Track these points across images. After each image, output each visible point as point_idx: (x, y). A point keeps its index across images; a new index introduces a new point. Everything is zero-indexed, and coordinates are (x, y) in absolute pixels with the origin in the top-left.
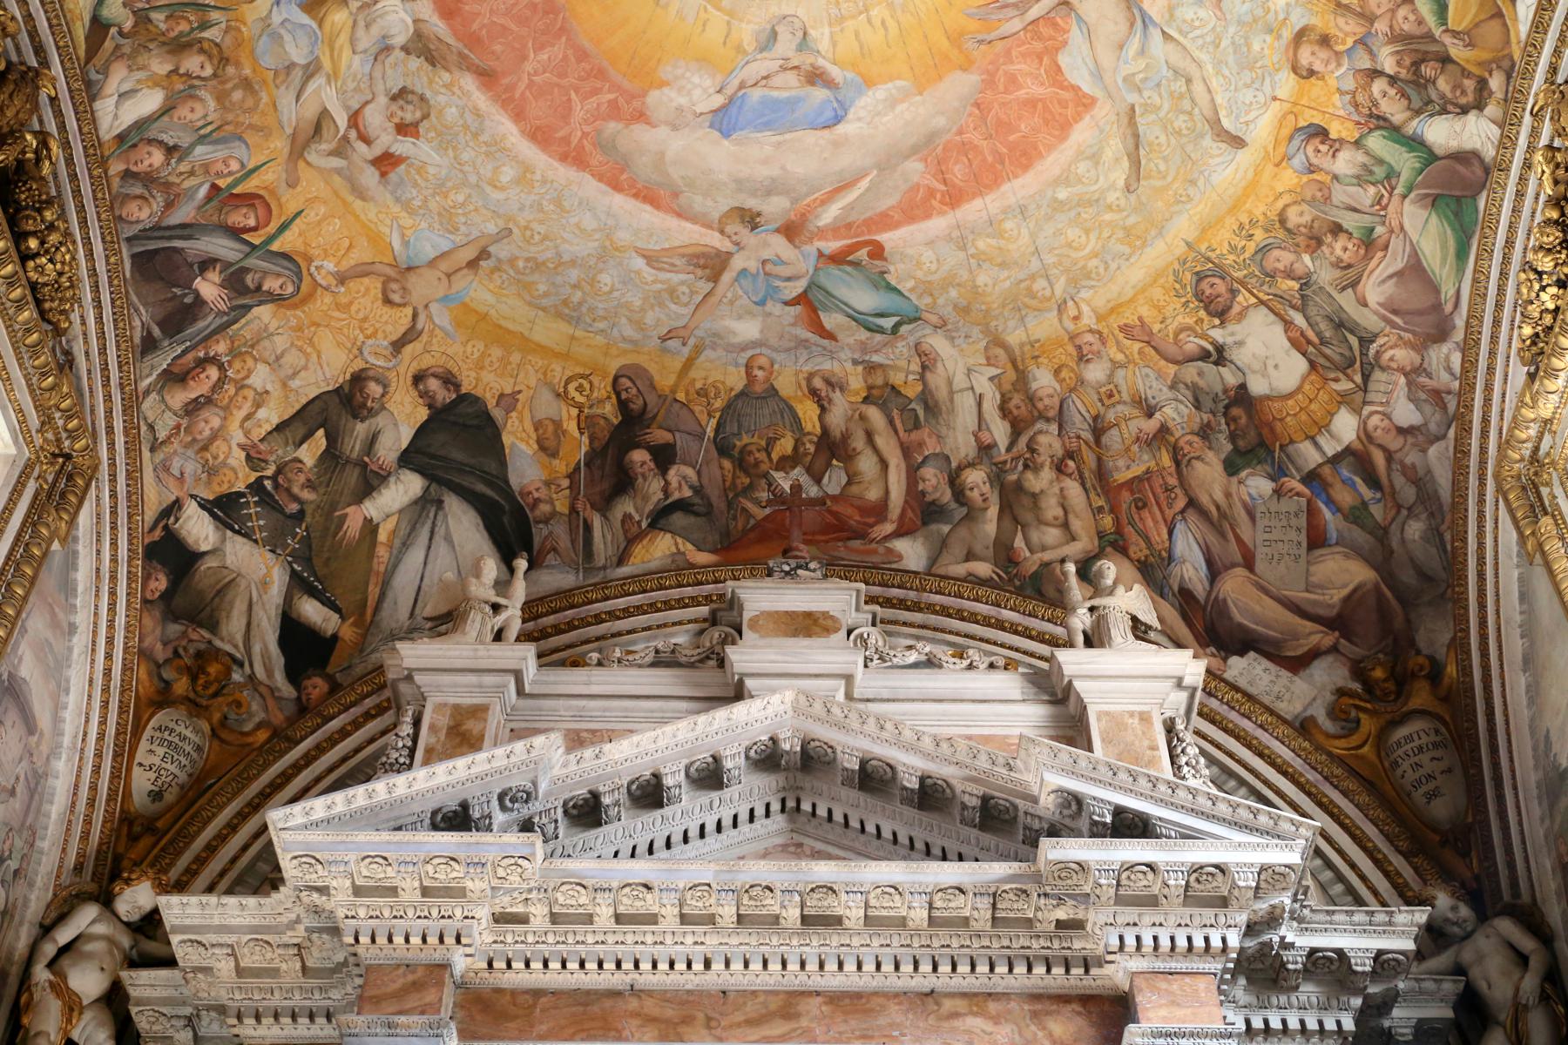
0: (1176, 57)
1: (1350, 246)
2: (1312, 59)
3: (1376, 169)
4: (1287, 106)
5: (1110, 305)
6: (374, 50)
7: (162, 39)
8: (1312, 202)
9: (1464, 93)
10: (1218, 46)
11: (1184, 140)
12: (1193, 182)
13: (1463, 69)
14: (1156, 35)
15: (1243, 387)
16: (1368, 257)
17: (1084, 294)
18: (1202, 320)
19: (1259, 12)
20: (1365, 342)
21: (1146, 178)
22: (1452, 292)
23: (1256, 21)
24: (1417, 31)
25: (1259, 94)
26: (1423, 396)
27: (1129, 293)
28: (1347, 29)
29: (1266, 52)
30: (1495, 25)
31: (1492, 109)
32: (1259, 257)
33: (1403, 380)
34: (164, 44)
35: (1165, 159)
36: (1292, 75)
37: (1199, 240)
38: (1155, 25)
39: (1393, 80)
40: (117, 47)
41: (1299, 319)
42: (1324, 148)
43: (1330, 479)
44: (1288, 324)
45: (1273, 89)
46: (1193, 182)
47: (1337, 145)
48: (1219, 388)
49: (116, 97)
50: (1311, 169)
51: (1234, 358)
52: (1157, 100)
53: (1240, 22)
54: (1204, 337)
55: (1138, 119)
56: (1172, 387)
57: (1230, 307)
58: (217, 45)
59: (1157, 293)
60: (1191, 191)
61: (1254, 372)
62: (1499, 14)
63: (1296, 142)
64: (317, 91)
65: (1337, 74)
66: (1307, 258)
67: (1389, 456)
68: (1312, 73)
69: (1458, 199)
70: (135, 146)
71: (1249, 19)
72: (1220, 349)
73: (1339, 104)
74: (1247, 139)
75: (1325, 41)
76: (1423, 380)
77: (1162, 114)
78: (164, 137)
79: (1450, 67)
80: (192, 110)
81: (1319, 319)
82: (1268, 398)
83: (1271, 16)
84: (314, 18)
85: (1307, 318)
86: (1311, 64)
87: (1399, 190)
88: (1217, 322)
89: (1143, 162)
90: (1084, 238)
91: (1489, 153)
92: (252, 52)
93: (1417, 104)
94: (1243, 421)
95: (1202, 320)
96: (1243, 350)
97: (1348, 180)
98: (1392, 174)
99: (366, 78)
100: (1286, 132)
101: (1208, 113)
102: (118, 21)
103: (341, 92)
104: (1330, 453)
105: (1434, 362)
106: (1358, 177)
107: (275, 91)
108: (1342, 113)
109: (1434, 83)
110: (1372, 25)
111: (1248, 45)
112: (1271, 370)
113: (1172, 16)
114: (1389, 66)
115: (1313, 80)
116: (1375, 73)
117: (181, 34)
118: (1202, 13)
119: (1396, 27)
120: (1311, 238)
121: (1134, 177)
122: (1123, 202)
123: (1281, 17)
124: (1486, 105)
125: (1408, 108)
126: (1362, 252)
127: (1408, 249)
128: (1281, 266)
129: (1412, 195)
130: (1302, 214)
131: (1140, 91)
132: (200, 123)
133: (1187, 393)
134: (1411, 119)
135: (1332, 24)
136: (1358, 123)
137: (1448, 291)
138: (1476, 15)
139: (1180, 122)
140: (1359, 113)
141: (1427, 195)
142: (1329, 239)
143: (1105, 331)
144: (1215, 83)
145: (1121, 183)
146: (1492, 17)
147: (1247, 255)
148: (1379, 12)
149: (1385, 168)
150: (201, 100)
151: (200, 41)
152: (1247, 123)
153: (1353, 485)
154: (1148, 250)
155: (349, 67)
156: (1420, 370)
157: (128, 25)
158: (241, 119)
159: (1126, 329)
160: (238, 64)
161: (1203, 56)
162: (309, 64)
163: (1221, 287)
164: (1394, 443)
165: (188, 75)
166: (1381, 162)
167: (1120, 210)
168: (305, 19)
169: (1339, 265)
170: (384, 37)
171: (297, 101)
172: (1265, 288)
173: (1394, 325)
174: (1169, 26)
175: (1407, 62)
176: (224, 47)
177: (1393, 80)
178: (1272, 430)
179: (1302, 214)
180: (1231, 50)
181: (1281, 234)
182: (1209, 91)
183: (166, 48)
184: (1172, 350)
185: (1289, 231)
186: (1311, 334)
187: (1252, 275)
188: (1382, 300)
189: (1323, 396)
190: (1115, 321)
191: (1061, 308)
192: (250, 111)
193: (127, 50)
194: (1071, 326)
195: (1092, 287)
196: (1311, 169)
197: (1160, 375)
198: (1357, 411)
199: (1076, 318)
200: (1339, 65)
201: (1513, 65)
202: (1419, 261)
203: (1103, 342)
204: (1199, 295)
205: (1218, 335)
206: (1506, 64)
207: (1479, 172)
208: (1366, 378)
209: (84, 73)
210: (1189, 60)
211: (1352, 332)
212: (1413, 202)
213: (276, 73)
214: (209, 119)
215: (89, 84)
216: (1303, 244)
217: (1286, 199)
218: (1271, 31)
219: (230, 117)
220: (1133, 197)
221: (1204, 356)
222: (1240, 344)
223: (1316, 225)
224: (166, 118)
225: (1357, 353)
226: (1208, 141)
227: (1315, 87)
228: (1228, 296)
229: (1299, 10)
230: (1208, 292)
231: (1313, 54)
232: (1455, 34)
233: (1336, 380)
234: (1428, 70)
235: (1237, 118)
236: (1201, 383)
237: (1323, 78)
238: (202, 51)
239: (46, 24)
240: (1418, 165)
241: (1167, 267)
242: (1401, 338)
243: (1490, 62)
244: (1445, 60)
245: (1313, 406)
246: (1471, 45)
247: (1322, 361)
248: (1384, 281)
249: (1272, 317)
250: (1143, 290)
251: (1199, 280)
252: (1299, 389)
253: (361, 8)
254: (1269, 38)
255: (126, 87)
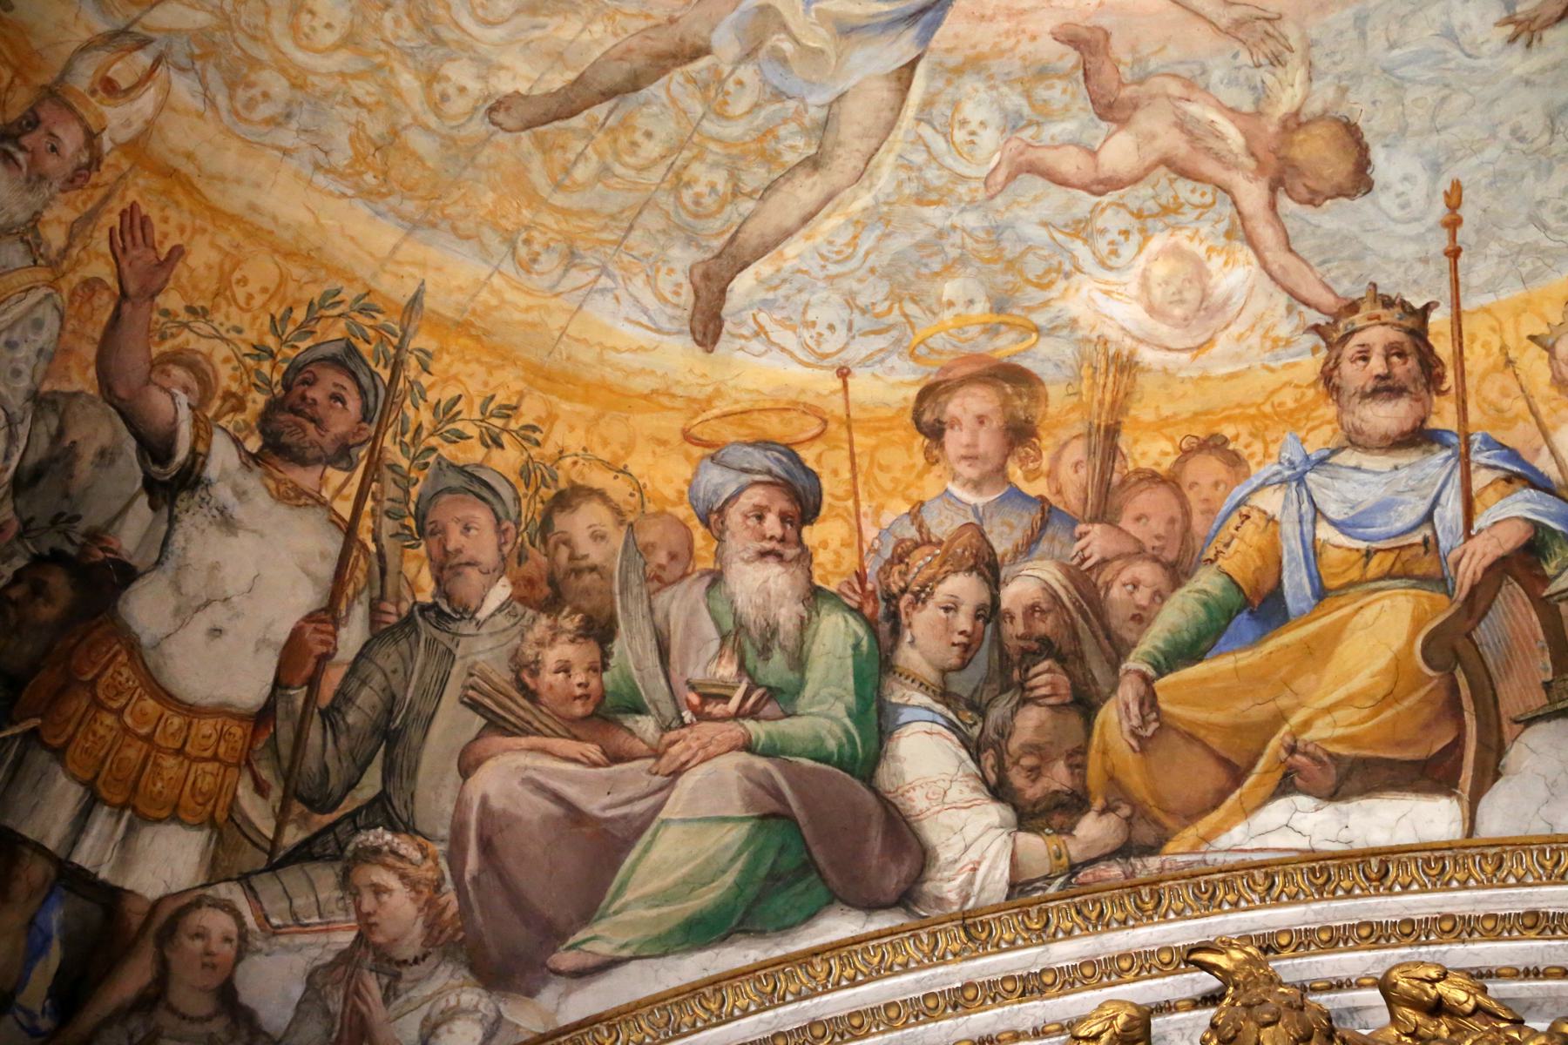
0: (858, 116)
1: (578, 677)
2: (968, 421)
3: (778, 658)
4: (836, 406)
5: (187, 168)
8: (636, 549)
9: (1035, 773)
10: (921, 201)
11: (667, 201)
12: (571, 259)
13: (1082, 750)
14: (902, 47)
15: (126, 574)
16: (574, 728)
17: (183, 88)
18: (240, 406)
19: (1034, 267)
20: (383, 811)
21: (540, 142)
22: (604, 949)
23: (1011, 265)
24: (1118, 618)
25: (842, 332)
26: (336, 1004)
27: (235, 200)
28: (1066, 472)
29: (947, 316)
30: (1210, 776)
31: (1035, 847)
32: (454, 480)
33: (345, 938)
35: (605, 171)
36: (913, 392)
37: (439, 324)
38: (924, 40)
39: (991, 612)
41: (352, 636)
42: (772, 524)
43: (19, 888)
44: (328, 615)
45: (866, 362)
46: (571, 259)
47: (791, 552)
48: (93, 517)
50: (713, 516)
51: (186, 520)
52: (739, 106)
53: (995, 233)
54: (203, 430)
55: (677, 75)
56: (40, 401)
57: (303, 462)
59: (261, 271)
60: (549, 262)
61: (177, 587)
62: (1237, 775)
63: (759, 459)
65: (956, 490)
66: (501, 592)
67: (154, 998)
68: (935, 433)
69: (808, 866)
71: (1011, 250)
72: (190, 479)
73: (887, 518)
74: (722, 347)
75: (1019, 434)
76: (373, 986)
77: (710, 127)
79: (1074, 721)
81: (378, 678)
82: (133, 647)
83: (1038, 296)
85: (364, 653)
86: (955, 423)
87: (757, 729)
88: (253, 444)
89: (577, 122)
90: (329, 38)
91: (947, 885)
93: (962, 684)
94: (47, 612)
95: (240, 406)
96: (214, 534)
97: (722, 608)
98: (782, 698)
100: (774, 427)
101: (752, 234)
104: (84, 856)
105: (428, 989)
106: (741, 627)
108: (870, 533)
109: (1024, 702)
110: (1094, 520)
111: (948, 270)
112: (203, 622)
113: (959, 71)
114: (1018, 591)
115: (920, 441)
116: (989, 569)
118: (989, 139)
119: (1107, 574)
120: (552, 582)
121: (531, 111)
122: (458, 105)
123: (1039, 319)
124: (1037, 831)
125: (944, 672)
126: (578, 709)
127: (639, 807)
128: (455, 539)
129: (761, 763)
130: (598, 537)
131: (749, 55)
133: (43, 443)
134: (924, 687)
135: (1064, 435)
136: (861, 577)
137: (602, 939)
138: (1210, 726)
139: (707, 177)
140: (885, 571)
141: (778, 795)
142: (570, 622)
143: (106, 175)
144: (830, 225)
145: (505, 85)
146: (1224, 762)
147: (447, 451)
148: (1126, 523)
149: (792, 677)
152: (760, 332)
153: (36, 951)
154: (361, 208)
156: (391, 967)
159: (134, 225)
161: (885, 177)
163: (342, 421)
164: (191, 995)
166: (799, 661)
167: (437, 105)
169: (523, 670)
172: (388, 525)
173: (456, 856)
174: (931, 75)
175: (1044, 627)
177: (991, 612)
178: (60, 693)
179: (598, 537)
180: (923, 233)
181: (531, 510)
182: (806, 220)
184: (133, 359)
185: (546, 525)
186: (333, 679)
187: (405, 483)
188: (497, 803)
189: (206, 776)
190: (139, 191)
191: (124, 39)
194: (84, 77)
195: (213, 104)
196: (713, 516)
197: (55, 357)
198: (215, 870)
199: (109, 87)
200: (977, 485)
201: (1153, 850)
202: (627, 844)
203: (78, 178)
204: (299, 374)
205: (222, 457)
206: (1145, 833)
207: (893, 881)
208: (304, 854)
210: (865, 146)
211: (388, 772)
212: (747, 772)
216: (529, 568)
217: (618, 489)
218: (999, 306)
220: (479, 127)
221: (156, 448)
222: (227, 523)
223: (588, 579)
225: (347, 806)
226: (682, 258)
227: (906, 453)
228: (328, 442)
229: (1068, 352)
230: (315, 393)
231: (981, 420)
232: (1149, 701)
233: (260, 788)
234: (1044, 676)
235: (766, 305)
236: (84, 467)
237: (932, 461)
240: (832, 745)
241: (339, 272)
242: (437, 886)
243: (1127, 798)
244: (1084, 704)
245: (169, 762)
246: (1143, 744)
247: (286, 733)
248: (540, 788)
249: (327, 570)
250: (254, 233)
251: (335, 362)
252: (192, 711)
254: (981, 308)
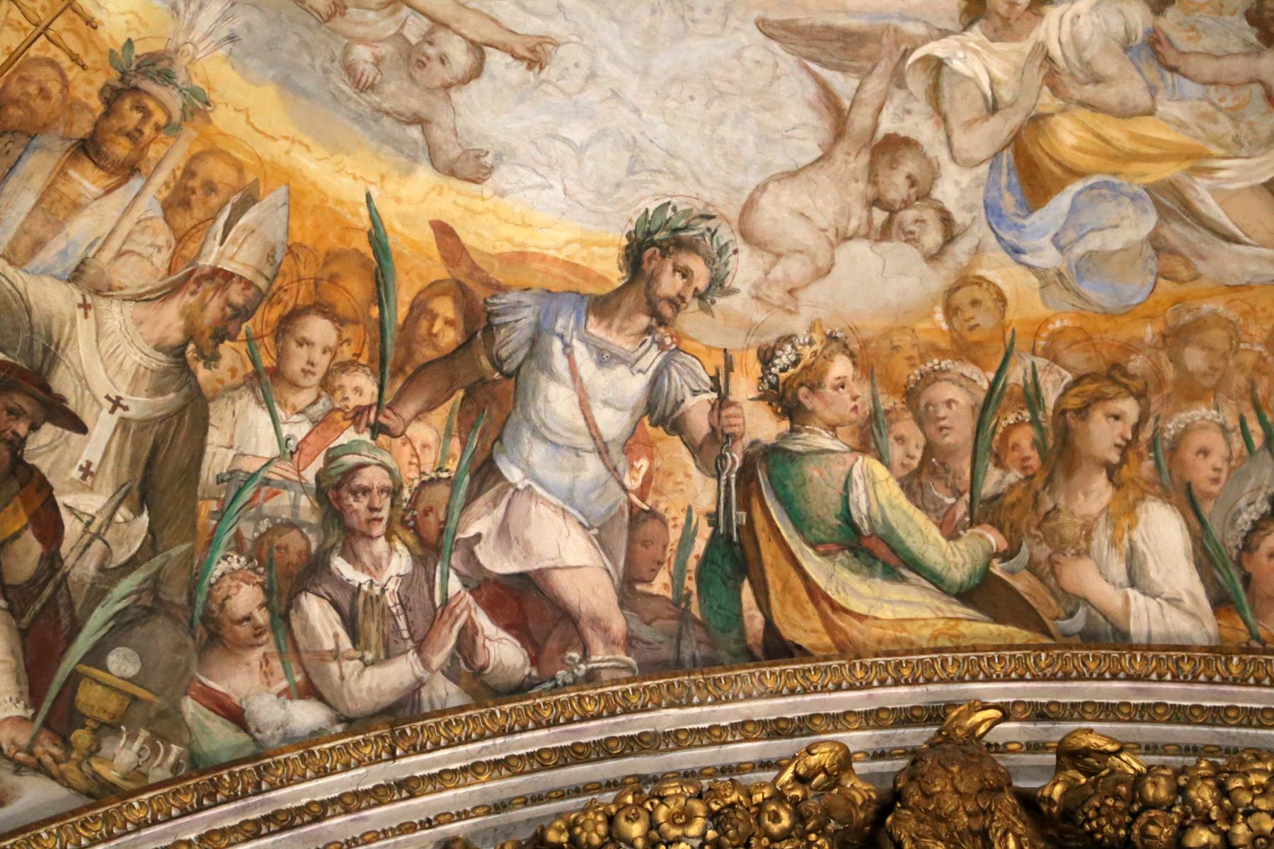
6: (1152, 72)
7: (1038, 482)
34: (1049, 480)
40: (1032, 567)
49: (1132, 593)
58: (1078, 381)
64: (1224, 198)
70: (1247, 580)
78: (1247, 518)
80: (1205, 452)
84: (1061, 185)
92: (1108, 315)
99: (1213, 93)
102: (980, 554)
103: (1235, 148)
107: (1203, 284)
117: (1038, 445)
132: (1238, 443)
150: (1187, 431)
151: (1060, 412)
155: (1181, 125)
157: (994, 539)
158: (1249, 359)
160: (1129, 348)
162: (1158, 205)
165: (1126, 448)
168: (1062, 202)
170: (1127, 47)
171: (1237, 241)
176: (1084, 368)
183: (1059, 477)
192: (1235, 334)
193: (1043, 552)
209: (1066, 641)
213: (1161, 274)
214: (1232, 422)
215: (1090, 638)
219: (1240, 380)
224: (1207, 508)
238: (1083, 412)
239: (903, 690)
253: (1055, 90)
255: (1118, 569)
